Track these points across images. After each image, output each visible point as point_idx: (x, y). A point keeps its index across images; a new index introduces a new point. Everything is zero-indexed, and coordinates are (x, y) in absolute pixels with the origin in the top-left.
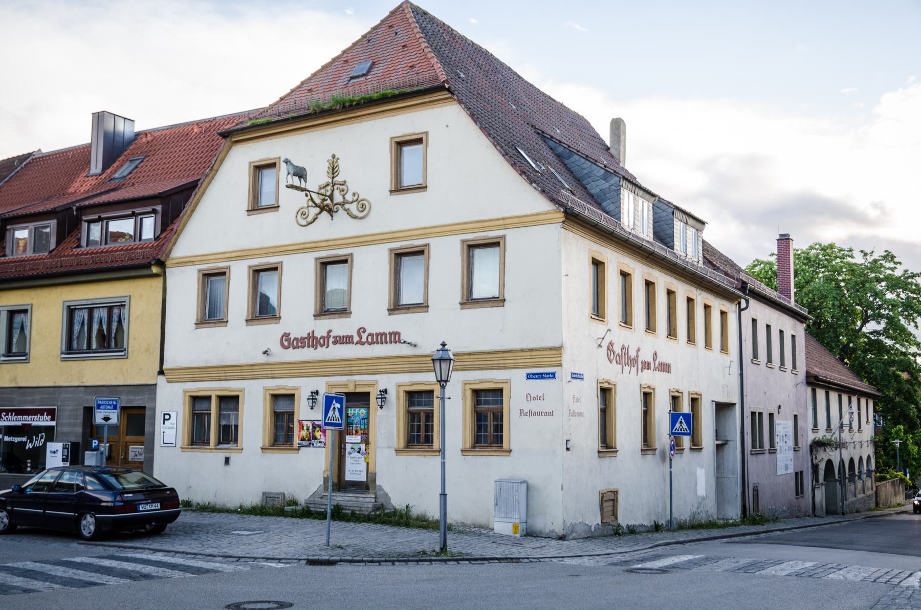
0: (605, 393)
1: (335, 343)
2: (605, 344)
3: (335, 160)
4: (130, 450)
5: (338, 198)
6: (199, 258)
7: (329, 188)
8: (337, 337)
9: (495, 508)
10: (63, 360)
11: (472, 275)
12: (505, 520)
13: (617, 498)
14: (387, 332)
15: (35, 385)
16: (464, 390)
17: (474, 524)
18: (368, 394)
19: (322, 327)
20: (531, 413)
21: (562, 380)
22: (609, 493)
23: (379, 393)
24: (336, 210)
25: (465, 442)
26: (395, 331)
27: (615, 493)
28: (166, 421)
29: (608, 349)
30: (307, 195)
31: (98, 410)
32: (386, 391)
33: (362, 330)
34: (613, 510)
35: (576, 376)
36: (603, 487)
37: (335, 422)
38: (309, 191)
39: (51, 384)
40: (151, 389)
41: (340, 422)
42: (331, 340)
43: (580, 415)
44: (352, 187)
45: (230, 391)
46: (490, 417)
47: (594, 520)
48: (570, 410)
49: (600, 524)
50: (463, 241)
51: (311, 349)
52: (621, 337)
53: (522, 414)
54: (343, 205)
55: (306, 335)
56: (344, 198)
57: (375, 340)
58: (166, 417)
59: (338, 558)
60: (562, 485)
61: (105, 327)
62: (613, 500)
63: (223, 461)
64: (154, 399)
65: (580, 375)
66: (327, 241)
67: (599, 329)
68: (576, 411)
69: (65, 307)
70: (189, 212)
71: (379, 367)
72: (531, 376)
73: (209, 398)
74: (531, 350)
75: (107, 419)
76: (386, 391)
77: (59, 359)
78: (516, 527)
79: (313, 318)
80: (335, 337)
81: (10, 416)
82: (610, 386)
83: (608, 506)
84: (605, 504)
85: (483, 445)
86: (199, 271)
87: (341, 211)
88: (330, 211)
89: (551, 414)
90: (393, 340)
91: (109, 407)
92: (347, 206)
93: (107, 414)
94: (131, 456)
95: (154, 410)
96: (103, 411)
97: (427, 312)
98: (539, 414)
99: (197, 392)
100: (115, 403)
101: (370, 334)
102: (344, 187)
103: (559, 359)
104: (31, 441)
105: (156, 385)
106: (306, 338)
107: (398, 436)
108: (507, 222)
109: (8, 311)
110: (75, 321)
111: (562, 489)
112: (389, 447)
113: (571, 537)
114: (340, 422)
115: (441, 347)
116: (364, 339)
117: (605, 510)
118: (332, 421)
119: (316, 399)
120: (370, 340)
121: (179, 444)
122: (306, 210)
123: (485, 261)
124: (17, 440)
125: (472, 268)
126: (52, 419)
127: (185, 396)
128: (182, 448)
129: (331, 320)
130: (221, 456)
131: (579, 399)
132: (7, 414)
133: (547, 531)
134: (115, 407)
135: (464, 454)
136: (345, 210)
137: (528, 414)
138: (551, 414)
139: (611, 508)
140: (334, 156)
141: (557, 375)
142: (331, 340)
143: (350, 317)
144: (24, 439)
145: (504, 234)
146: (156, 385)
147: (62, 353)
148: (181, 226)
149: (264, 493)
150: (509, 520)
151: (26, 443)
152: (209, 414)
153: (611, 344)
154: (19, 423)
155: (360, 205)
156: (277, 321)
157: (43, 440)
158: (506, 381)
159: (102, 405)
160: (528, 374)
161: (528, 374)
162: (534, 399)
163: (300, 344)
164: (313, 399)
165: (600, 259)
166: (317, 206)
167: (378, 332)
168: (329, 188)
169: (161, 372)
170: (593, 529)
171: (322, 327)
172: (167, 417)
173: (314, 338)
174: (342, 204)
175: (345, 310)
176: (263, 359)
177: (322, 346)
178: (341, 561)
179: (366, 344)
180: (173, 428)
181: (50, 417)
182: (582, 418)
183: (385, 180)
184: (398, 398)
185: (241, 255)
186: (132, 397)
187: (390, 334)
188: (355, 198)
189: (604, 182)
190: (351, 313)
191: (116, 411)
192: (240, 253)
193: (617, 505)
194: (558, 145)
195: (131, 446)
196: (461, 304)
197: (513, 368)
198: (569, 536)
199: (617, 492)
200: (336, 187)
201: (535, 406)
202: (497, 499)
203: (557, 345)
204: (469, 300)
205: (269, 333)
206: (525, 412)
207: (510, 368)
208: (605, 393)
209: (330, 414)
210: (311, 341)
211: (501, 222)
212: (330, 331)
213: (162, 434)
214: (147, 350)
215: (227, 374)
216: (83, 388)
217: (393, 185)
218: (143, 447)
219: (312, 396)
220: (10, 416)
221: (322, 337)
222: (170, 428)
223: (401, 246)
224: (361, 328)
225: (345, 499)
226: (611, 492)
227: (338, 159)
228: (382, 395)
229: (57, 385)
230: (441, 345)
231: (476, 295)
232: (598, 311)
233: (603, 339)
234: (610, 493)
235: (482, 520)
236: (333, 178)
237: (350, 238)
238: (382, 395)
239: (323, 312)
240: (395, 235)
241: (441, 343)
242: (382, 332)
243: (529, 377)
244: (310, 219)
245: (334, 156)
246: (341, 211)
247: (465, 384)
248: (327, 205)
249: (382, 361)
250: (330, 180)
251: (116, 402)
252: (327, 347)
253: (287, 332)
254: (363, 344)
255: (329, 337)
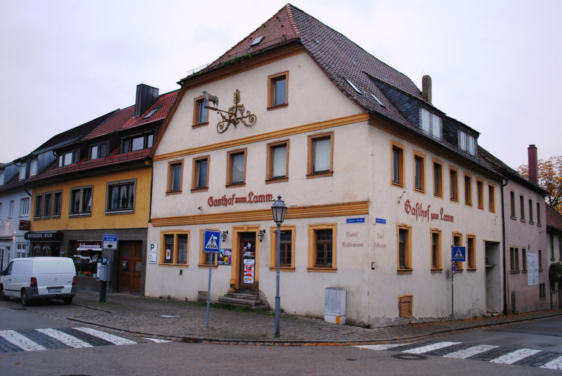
0: (404, 233)
1: (236, 202)
2: (403, 201)
3: (238, 93)
4: (137, 265)
5: (239, 115)
6: (168, 155)
7: (234, 110)
8: (238, 198)
9: (325, 306)
10: (107, 215)
11: (315, 157)
12: (331, 314)
13: (412, 301)
14: (265, 195)
15: (94, 228)
16: (309, 230)
17: (314, 316)
18: (255, 233)
19: (230, 192)
20: (349, 245)
21: (368, 223)
22: (405, 298)
23: (260, 232)
24: (237, 122)
25: (309, 264)
26: (269, 194)
27: (411, 297)
28: (152, 249)
29: (406, 205)
30: (218, 113)
31: (104, 241)
32: (264, 231)
33: (251, 194)
34: (409, 309)
35: (381, 221)
36: (402, 294)
37: (213, 248)
38: (220, 111)
39: (101, 228)
40: (145, 230)
41: (217, 248)
42: (235, 200)
43: (384, 246)
44: (247, 108)
45: (183, 232)
46: (326, 247)
47: (394, 314)
48: (375, 243)
49: (398, 317)
50: (309, 136)
51: (224, 206)
52: (415, 198)
53: (344, 245)
54: (242, 119)
55: (221, 198)
56: (242, 115)
57: (258, 200)
58: (152, 247)
59: (202, 338)
60: (368, 292)
61: (125, 196)
62: (409, 302)
63: (179, 272)
64: (146, 236)
65: (383, 220)
66: (233, 141)
67: (398, 191)
68: (379, 244)
69: (108, 186)
70: (163, 129)
71: (260, 216)
72: (349, 221)
73: (172, 236)
74: (349, 204)
75: (110, 246)
76: (264, 231)
77: (104, 215)
78: (338, 318)
79: (225, 187)
80: (237, 199)
81: (83, 245)
82: (408, 229)
83: (405, 306)
84: (402, 305)
85: (321, 265)
86: (169, 162)
87: (241, 123)
88: (235, 124)
89: (362, 245)
90: (268, 199)
91: (111, 240)
92: (244, 120)
93: (110, 243)
94: (137, 268)
95: (146, 242)
96: (108, 242)
97: (288, 181)
98: (354, 245)
99: (167, 232)
100: (115, 237)
101: (256, 197)
102: (242, 108)
103: (366, 209)
104: (92, 259)
105: (147, 228)
106: (221, 200)
107: (271, 259)
108: (335, 122)
109: (84, 189)
110: (113, 194)
111: (368, 295)
112: (266, 266)
113: (375, 326)
114: (217, 248)
115: (278, 199)
116: (252, 200)
117: (403, 308)
118: (211, 248)
119: (226, 236)
120: (255, 200)
121: (158, 262)
122: (222, 124)
123: (322, 149)
124: (86, 258)
125: (315, 153)
126: (101, 247)
127: (161, 234)
128: (159, 264)
129: (235, 188)
130: (178, 269)
131: (383, 236)
132: (82, 244)
133: (359, 322)
134: (115, 240)
135: (309, 271)
136: (243, 122)
137: (347, 246)
138: (362, 245)
139: (408, 307)
140: (237, 91)
141: (366, 220)
142: (235, 200)
143: (245, 186)
144: (89, 258)
145: (333, 130)
146: (147, 228)
147: (106, 211)
148: (160, 137)
149: (200, 292)
150: (333, 314)
151: (89, 260)
152: (173, 245)
153: (408, 201)
154: (87, 249)
155: (251, 118)
156: (206, 190)
157: (97, 258)
158: (334, 224)
159: (107, 238)
160: (347, 220)
161: (347, 220)
162: (351, 235)
163: (218, 203)
164: (224, 236)
165: (399, 146)
166: (226, 121)
167: (260, 195)
168: (234, 110)
169: (150, 221)
170: (393, 321)
171: (230, 192)
172: (153, 246)
173: (226, 199)
174: (241, 119)
175: (243, 182)
176: (198, 212)
177: (230, 204)
178: (204, 340)
179: (253, 202)
180: (155, 253)
181: (100, 246)
182: (384, 248)
183: (265, 103)
184: (271, 235)
185: (189, 152)
186: (136, 235)
187: (267, 196)
188: (248, 114)
189: (409, 104)
190: (245, 184)
191: (116, 242)
192: (188, 151)
193: (412, 305)
194: (381, 84)
195: (137, 263)
196: (307, 175)
197: (339, 216)
198: (373, 325)
199: (412, 296)
200: (238, 109)
201: (352, 240)
202: (326, 301)
203: (365, 200)
204: (313, 173)
205: (202, 197)
206: (345, 244)
207: (337, 216)
208: (404, 233)
209: (209, 243)
210: (224, 201)
211: (331, 123)
212: (234, 195)
213: (150, 256)
214: (144, 209)
215: (181, 222)
216: (114, 231)
217: (269, 104)
218: (141, 263)
219: (224, 234)
220: (83, 245)
221: (230, 199)
222: (154, 253)
223: (274, 142)
224: (251, 193)
225: (240, 298)
226: (407, 296)
227: (239, 92)
228: (261, 233)
229: (103, 228)
230: (278, 197)
231: (317, 169)
232: (398, 181)
233: (401, 197)
234: (407, 298)
235: (318, 313)
236: (237, 103)
237: (245, 138)
238: (261, 233)
239: (231, 184)
240: (270, 135)
241: (278, 196)
242: (262, 194)
243: (348, 221)
244: (224, 129)
245: (237, 91)
246: (241, 123)
247: (310, 226)
248: (233, 120)
249: (262, 213)
250: (235, 105)
251: (116, 237)
252: (232, 205)
253: (212, 196)
254: (251, 202)
255: (233, 198)
